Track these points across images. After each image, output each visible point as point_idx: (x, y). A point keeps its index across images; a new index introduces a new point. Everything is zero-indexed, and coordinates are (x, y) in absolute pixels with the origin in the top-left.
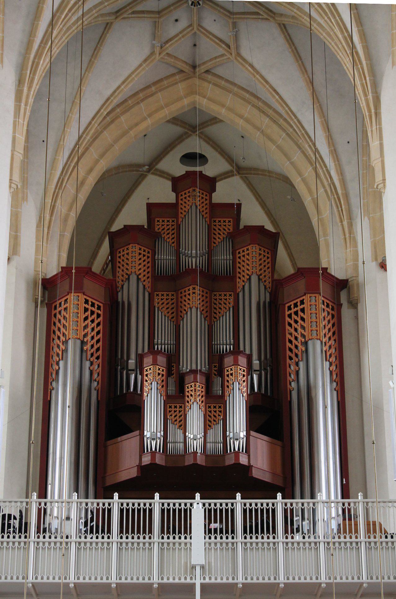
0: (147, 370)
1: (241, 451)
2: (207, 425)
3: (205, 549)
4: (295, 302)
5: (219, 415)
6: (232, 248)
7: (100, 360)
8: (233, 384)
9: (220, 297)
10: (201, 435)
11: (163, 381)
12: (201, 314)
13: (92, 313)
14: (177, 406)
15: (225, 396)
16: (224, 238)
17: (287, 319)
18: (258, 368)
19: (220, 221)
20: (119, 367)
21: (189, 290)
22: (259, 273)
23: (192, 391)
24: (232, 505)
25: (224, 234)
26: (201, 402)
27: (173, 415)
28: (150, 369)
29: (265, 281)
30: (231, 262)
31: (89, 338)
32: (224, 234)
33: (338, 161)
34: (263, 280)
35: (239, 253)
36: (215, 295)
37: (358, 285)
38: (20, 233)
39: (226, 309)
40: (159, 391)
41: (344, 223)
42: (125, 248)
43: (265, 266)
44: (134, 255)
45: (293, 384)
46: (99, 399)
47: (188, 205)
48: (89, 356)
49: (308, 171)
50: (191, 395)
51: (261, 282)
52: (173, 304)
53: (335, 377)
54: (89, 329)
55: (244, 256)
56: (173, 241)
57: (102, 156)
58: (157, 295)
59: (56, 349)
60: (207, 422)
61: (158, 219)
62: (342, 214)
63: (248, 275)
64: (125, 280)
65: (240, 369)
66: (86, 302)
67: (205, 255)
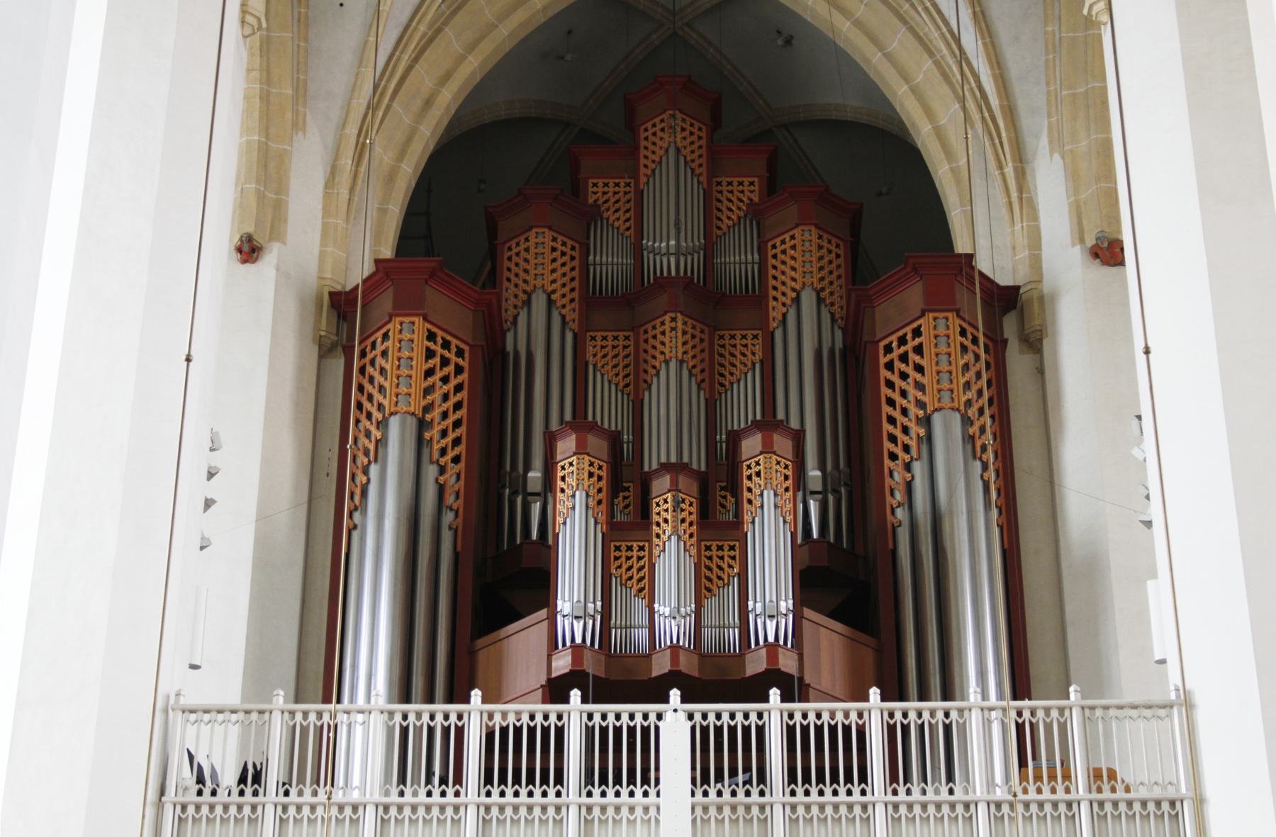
0: (563, 468)
1: (781, 642)
2: (705, 585)
3: (694, 821)
4: (900, 333)
5: (730, 566)
6: (759, 236)
7: (462, 465)
8: (762, 495)
9: (733, 342)
10: (688, 608)
11: (600, 490)
12: (691, 374)
13: (445, 362)
14: (632, 546)
15: (743, 523)
16: (739, 218)
17: (884, 373)
18: (819, 488)
19: (730, 184)
20: (508, 490)
21: (663, 323)
22: (819, 286)
23: (667, 510)
24: (760, 716)
25: (739, 209)
26: (687, 536)
27: (624, 567)
28: (571, 464)
29: (832, 304)
30: (756, 267)
31: (436, 414)
32: (739, 209)
33: (990, 37)
34: (828, 302)
35: (774, 247)
36: (721, 337)
37: (1041, 298)
38: (288, 196)
39: (746, 365)
40: (590, 512)
41: (1006, 170)
42: (522, 239)
43: (831, 272)
44: (540, 249)
45: (901, 514)
46: (459, 549)
47: (661, 148)
48: (436, 455)
49: (925, 68)
50: (666, 521)
51: (823, 306)
52: (627, 356)
54: (437, 396)
55: (784, 252)
56: (628, 224)
57: (471, 47)
58: (593, 338)
59: (363, 441)
60: (703, 580)
61: (595, 181)
62: (1000, 151)
63: (793, 290)
64: (520, 304)
65: (778, 463)
66: (431, 337)
67: (699, 253)
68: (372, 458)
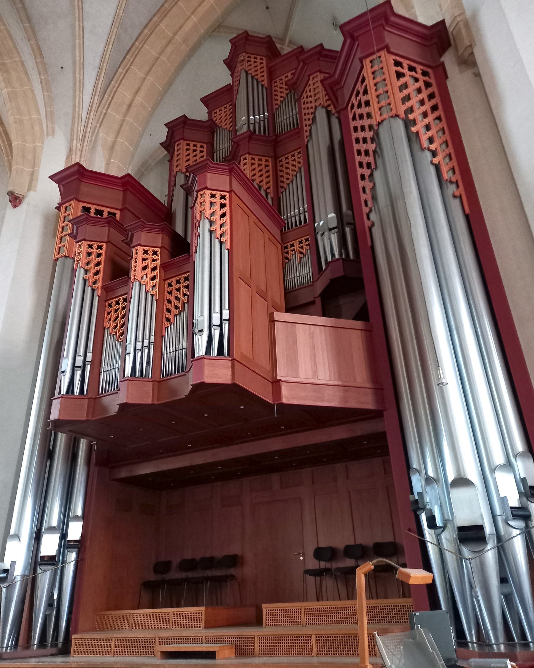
16: (287, 94)
38: (39, 167)
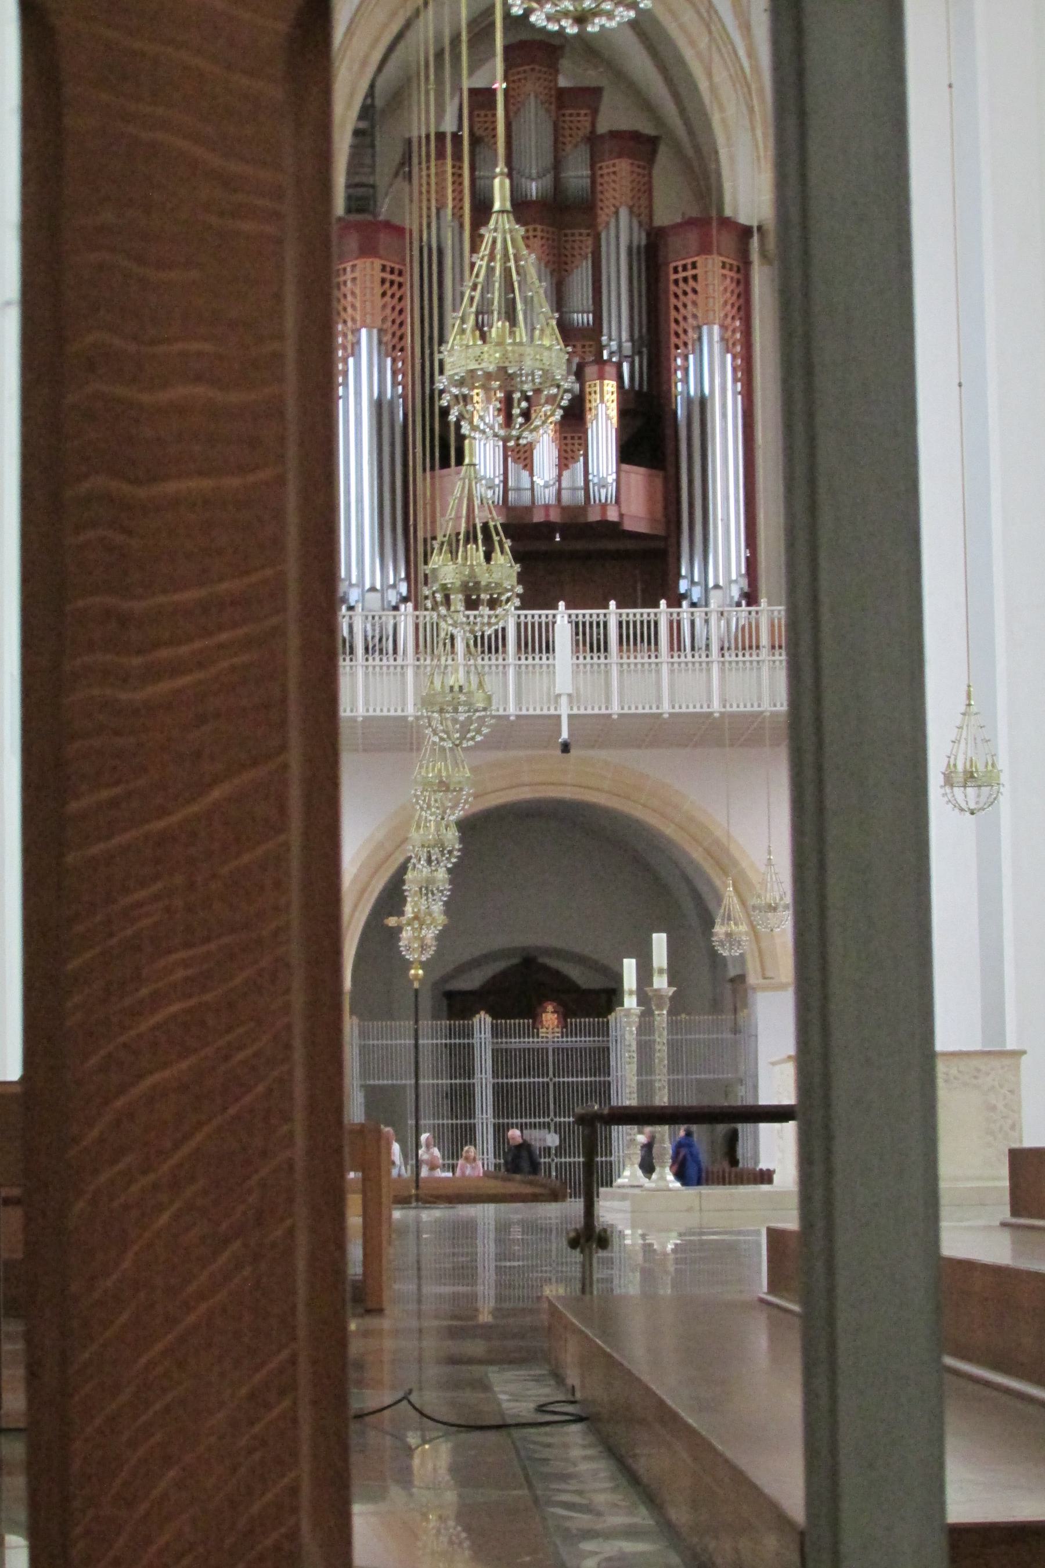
4: (684, 262)
13: (392, 283)
53: (739, 374)
63: (614, 206)
66: (384, 268)
68: (349, 350)
